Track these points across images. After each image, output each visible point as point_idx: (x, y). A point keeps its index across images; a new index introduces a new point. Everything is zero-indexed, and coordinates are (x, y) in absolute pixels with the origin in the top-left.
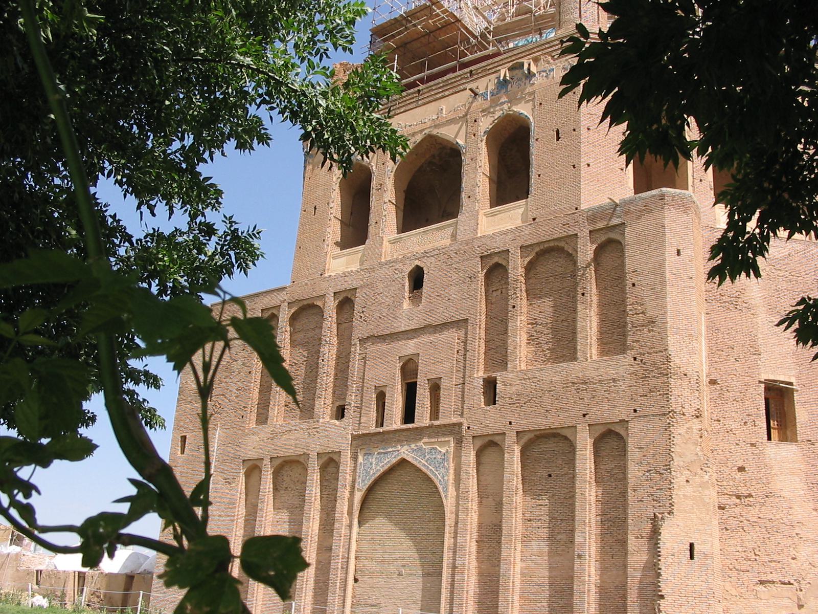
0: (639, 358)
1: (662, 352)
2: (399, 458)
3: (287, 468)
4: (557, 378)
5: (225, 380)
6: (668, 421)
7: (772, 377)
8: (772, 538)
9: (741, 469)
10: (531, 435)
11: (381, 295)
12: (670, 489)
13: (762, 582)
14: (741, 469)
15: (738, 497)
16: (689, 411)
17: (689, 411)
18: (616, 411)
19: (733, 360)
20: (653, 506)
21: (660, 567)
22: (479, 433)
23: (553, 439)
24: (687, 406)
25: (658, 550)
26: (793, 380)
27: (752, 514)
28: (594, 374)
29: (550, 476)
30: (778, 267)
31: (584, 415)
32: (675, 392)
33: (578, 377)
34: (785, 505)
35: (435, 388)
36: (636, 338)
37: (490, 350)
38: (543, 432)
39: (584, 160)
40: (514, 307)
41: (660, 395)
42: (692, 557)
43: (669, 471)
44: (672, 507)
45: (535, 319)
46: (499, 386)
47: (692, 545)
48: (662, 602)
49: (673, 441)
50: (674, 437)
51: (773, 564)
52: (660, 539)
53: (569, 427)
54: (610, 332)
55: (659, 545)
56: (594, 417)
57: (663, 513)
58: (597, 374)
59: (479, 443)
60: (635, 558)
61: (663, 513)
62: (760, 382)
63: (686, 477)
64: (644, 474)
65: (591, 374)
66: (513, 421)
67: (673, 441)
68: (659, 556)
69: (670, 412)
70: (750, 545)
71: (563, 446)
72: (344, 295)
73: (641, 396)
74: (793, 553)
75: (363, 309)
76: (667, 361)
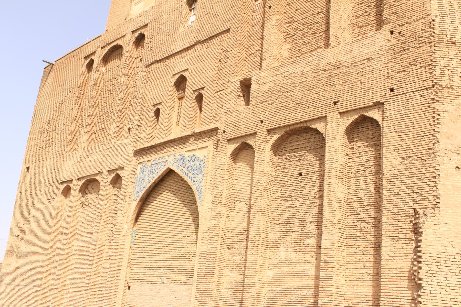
0: (396, 32)
1: (424, 18)
2: (165, 168)
3: (90, 187)
4: (309, 69)
5: (56, 119)
6: (432, 97)
11: (165, 25)
12: (434, 177)
18: (370, 93)
20: (413, 201)
21: (420, 276)
22: (233, 135)
23: (305, 135)
25: (419, 254)
28: (345, 58)
29: (300, 174)
31: (335, 103)
32: (441, 62)
33: (329, 64)
35: (199, 99)
36: (394, 10)
37: (250, 55)
38: (292, 127)
40: (270, 7)
41: (421, 67)
43: (433, 155)
44: (438, 201)
45: (291, 18)
46: (253, 87)
49: (438, 119)
50: (439, 115)
52: (420, 241)
53: (319, 118)
54: (367, 14)
55: (419, 249)
56: (345, 103)
57: (426, 208)
58: (350, 56)
59: (232, 147)
60: (391, 266)
61: (426, 208)
63: (456, 163)
64: (402, 162)
65: (343, 58)
67: (438, 119)
68: (420, 262)
69: (433, 86)
71: (314, 142)
72: (139, 32)
73: (398, 72)
75: (151, 40)
76: (430, 27)
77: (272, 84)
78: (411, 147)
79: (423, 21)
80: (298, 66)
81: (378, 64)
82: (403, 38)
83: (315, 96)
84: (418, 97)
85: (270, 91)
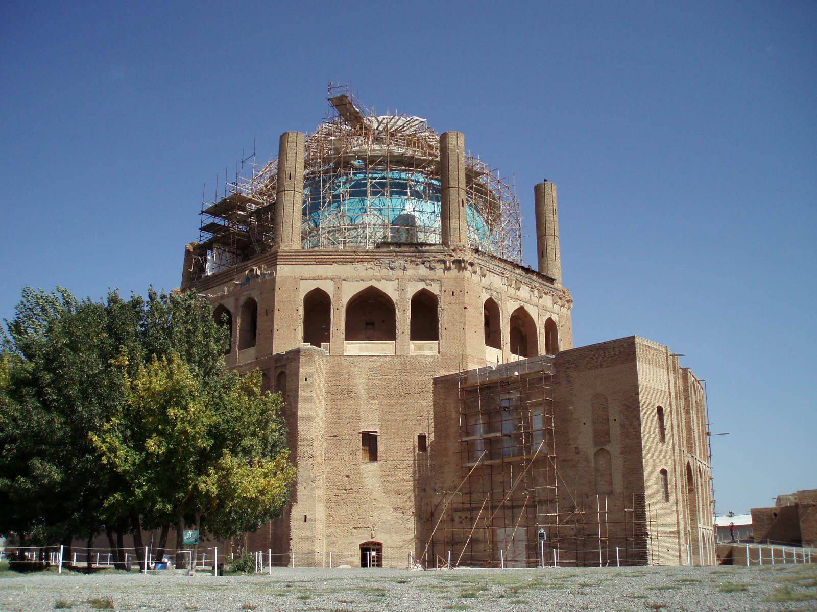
9: (348, 476)
13: (355, 528)
14: (348, 476)
15: (346, 490)
16: (307, 455)
17: (307, 455)
24: (306, 453)
26: (377, 430)
27: (352, 497)
30: (375, 372)
34: (369, 491)
39: (275, 327)
42: (305, 521)
47: (306, 516)
48: (291, 541)
62: (360, 433)
70: (350, 511)
74: (371, 513)
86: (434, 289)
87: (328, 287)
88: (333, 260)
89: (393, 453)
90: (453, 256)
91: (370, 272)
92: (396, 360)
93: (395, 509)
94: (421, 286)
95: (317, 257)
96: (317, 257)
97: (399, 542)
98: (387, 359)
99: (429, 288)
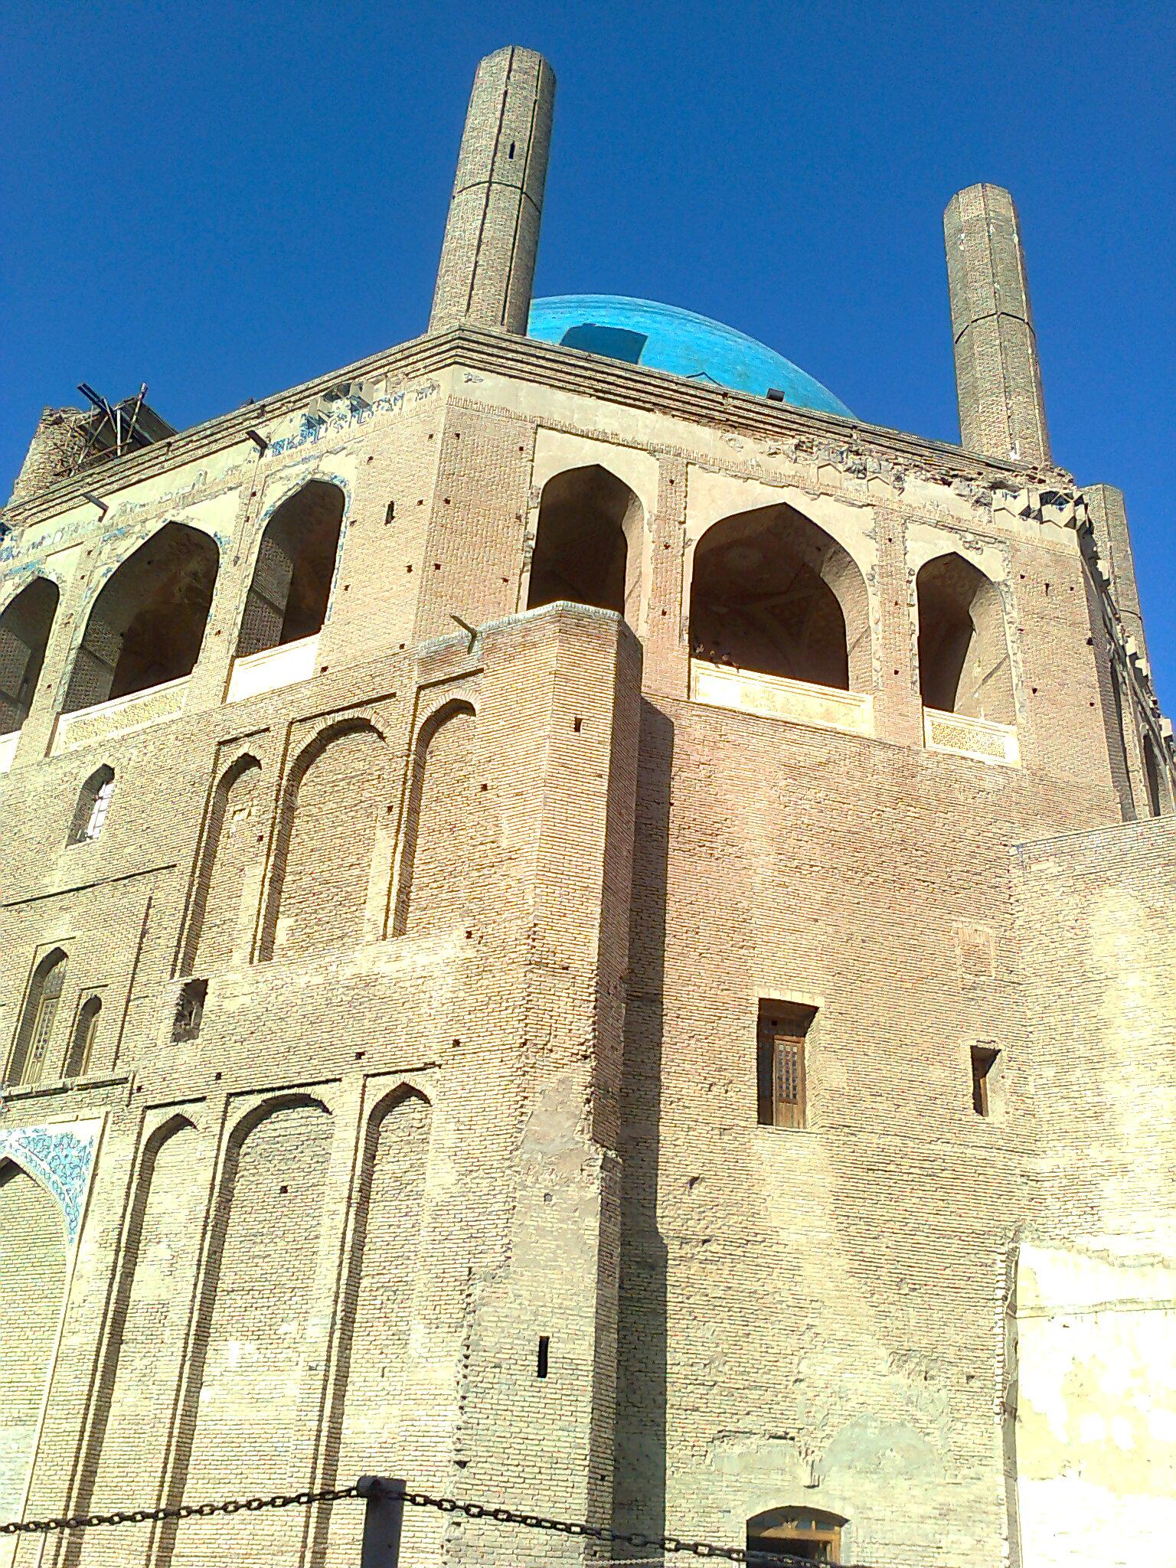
0: (476, 935)
7: (775, 995)
8: (755, 1336)
10: (255, 1101)
19: (695, 955)
26: (818, 1002)
29: (284, 1190)
31: (359, 1055)
33: (358, 976)
42: (542, 1372)
47: (544, 1343)
51: (755, 1394)
54: (435, 885)
66: (223, 1070)
77: (247, 1000)
78: (477, 1153)
79: (519, 922)
80: (301, 971)
81: (443, 988)
82: (485, 949)
83: (325, 1036)
84: (496, 1062)
85: (243, 1011)
86: (988, 562)
87: (637, 473)
88: (653, 399)
89: (883, 1105)
90: (1041, 481)
91: (783, 466)
92: (879, 755)
93: (901, 1357)
94: (946, 544)
95: (599, 376)
96: (599, 376)
97: (923, 1518)
98: (853, 748)
99: (971, 556)
